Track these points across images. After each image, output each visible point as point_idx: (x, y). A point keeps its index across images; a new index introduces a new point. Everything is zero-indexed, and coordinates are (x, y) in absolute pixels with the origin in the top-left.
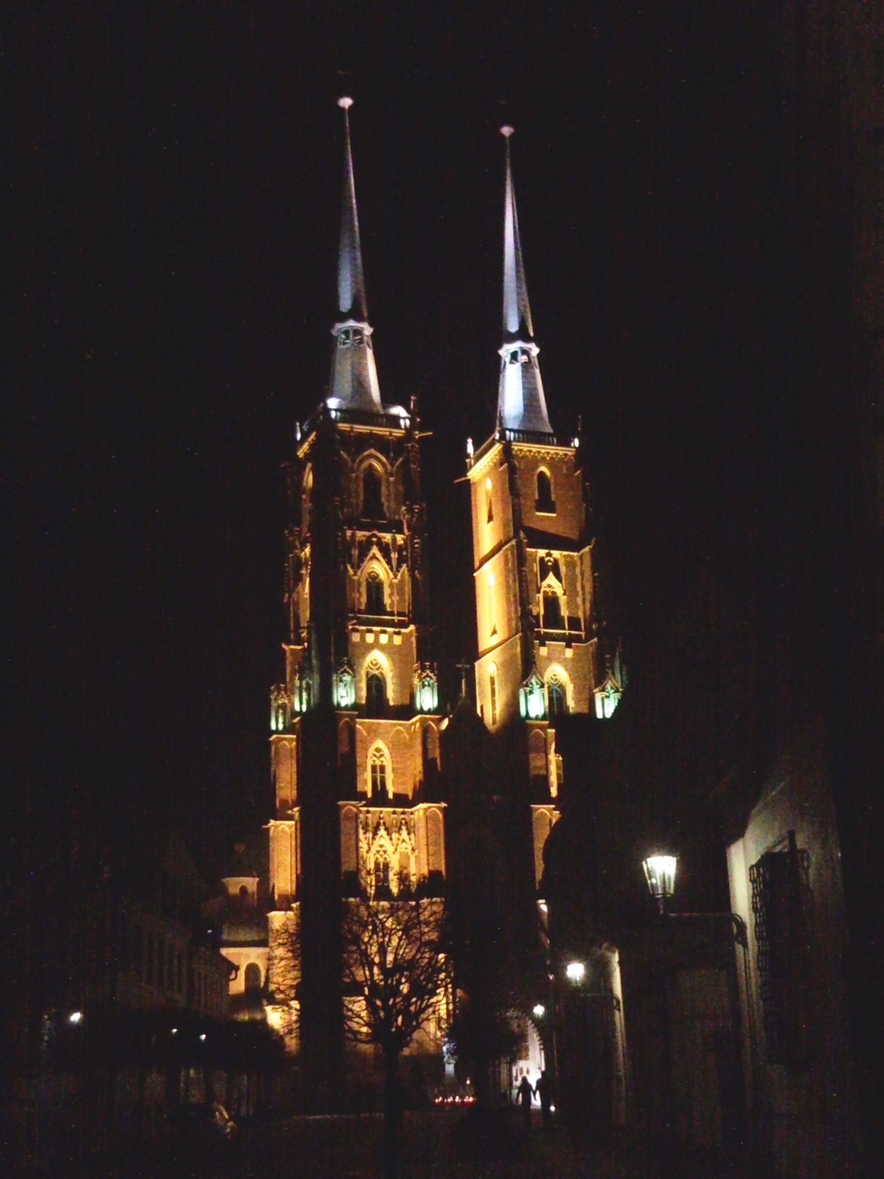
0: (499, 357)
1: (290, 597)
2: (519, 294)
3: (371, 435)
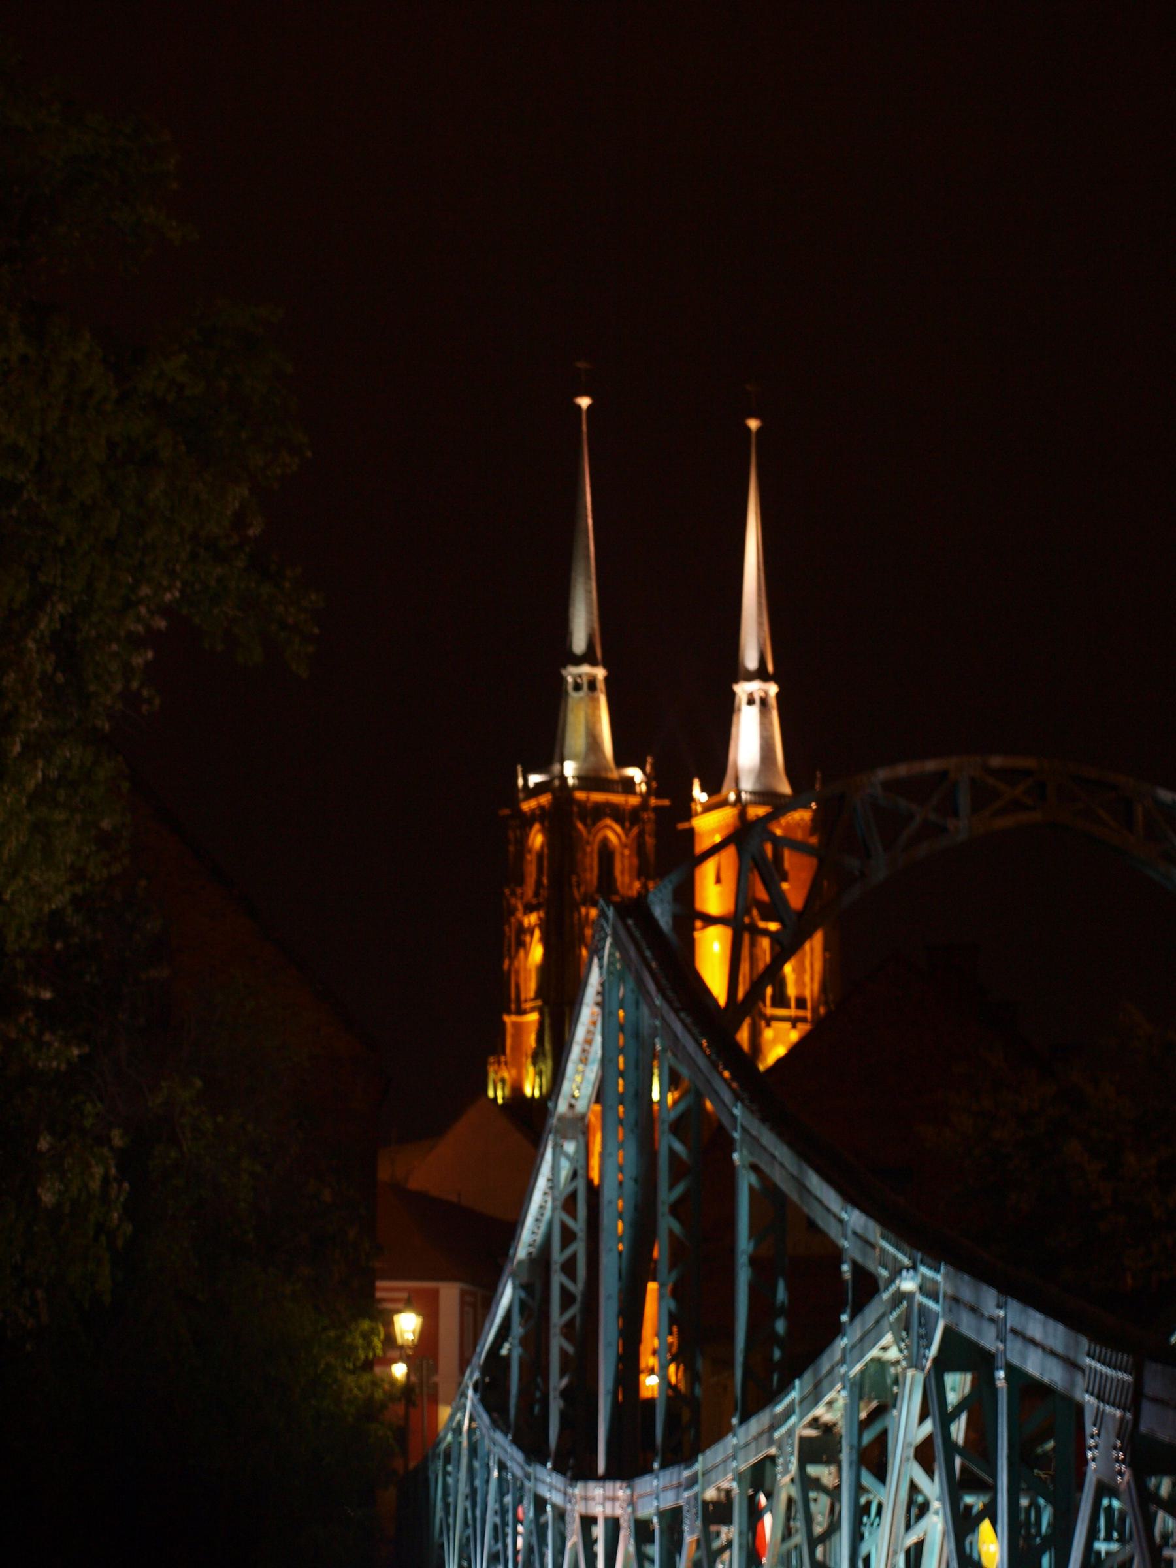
0: (733, 694)
1: (510, 965)
2: (760, 624)
3: (608, 804)
